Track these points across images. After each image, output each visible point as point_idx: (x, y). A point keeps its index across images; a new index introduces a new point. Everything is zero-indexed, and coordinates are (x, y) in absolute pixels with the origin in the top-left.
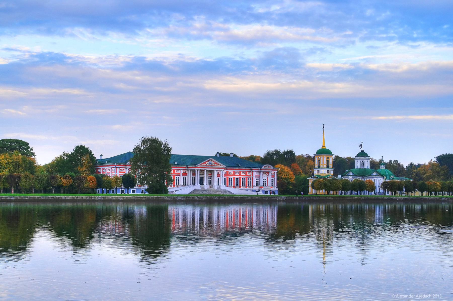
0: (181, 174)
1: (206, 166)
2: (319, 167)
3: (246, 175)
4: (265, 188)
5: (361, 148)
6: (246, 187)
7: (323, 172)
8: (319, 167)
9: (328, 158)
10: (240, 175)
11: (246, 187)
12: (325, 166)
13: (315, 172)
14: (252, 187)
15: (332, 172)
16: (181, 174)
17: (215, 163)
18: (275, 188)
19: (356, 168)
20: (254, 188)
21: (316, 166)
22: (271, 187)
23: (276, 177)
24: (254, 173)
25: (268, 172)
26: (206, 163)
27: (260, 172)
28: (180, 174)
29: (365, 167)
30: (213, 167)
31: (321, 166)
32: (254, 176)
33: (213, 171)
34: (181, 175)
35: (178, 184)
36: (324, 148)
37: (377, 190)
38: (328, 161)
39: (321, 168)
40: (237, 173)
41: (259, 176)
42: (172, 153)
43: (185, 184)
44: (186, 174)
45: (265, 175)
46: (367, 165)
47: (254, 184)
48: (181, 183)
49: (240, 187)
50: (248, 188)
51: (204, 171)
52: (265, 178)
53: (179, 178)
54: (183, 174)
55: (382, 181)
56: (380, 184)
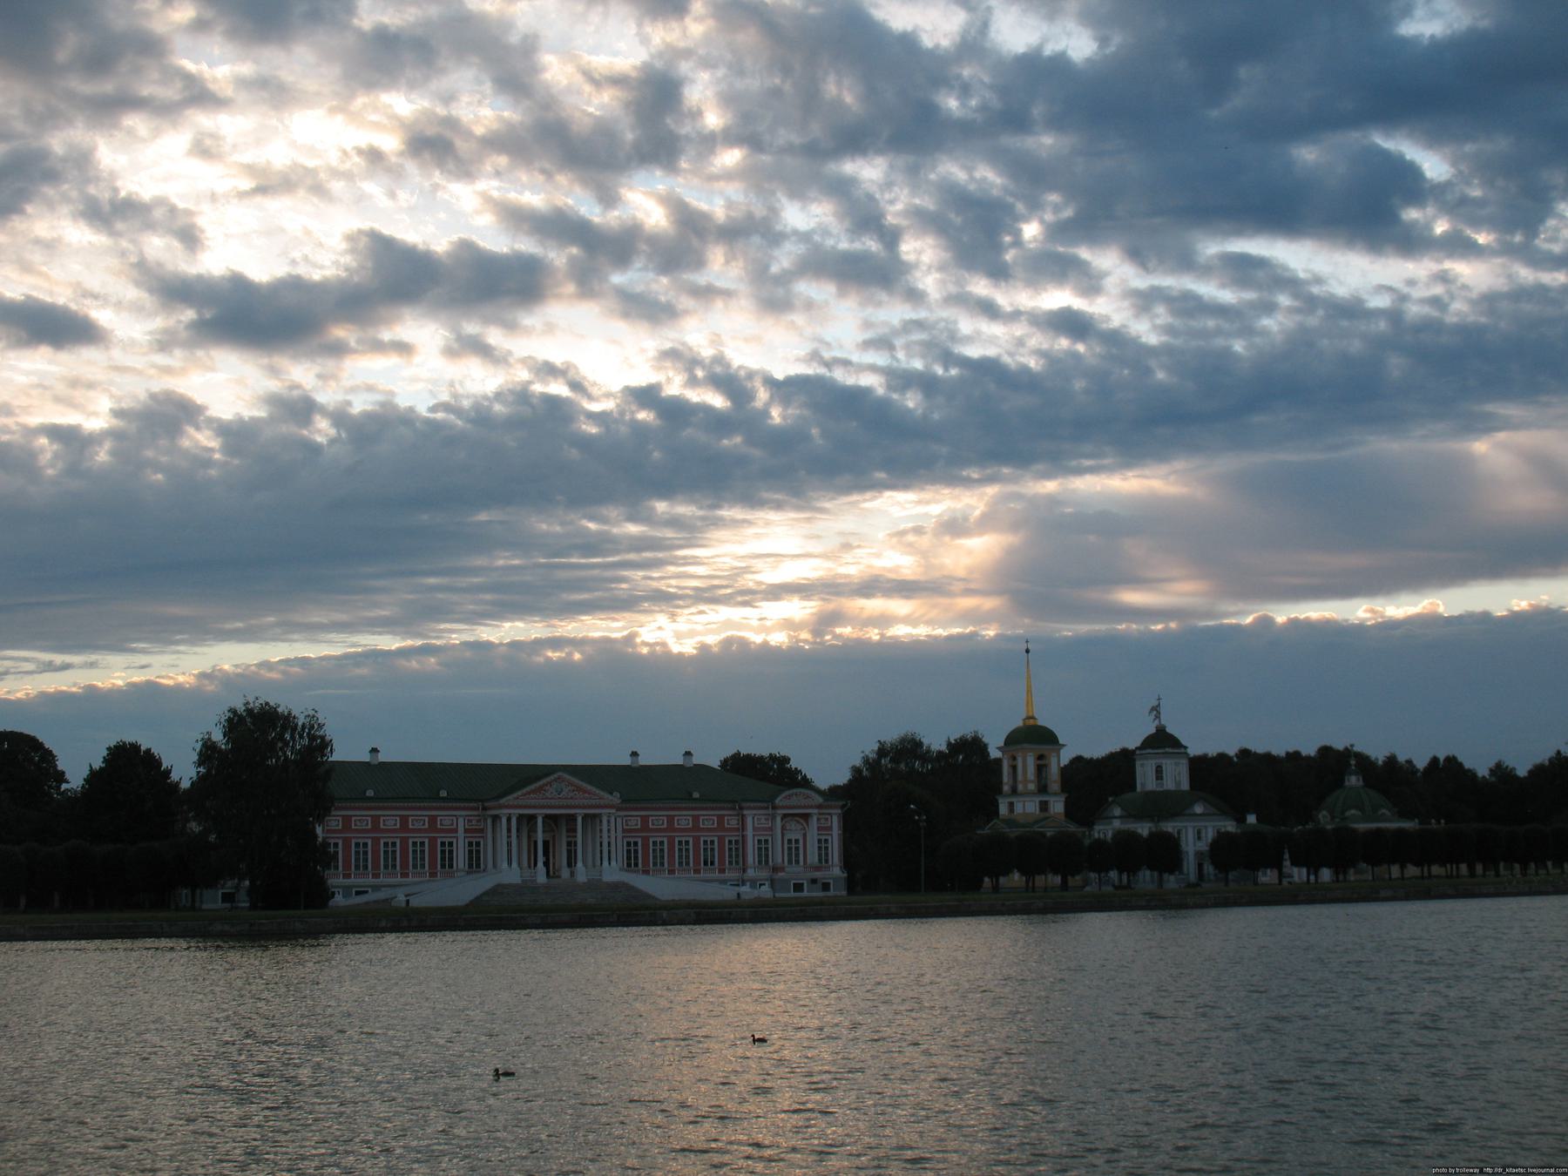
0: (461, 829)
1: (543, 802)
2: (1014, 791)
4: (794, 872)
5: (1158, 717)
6: (722, 871)
7: (1027, 807)
8: (1014, 791)
9: (1041, 757)
10: (696, 828)
11: (722, 871)
12: (1032, 787)
13: (1003, 809)
14: (744, 871)
15: (1058, 806)
16: (461, 829)
17: (579, 789)
18: (837, 871)
19: (1139, 789)
20: (751, 873)
21: (1006, 788)
22: (818, 869)
23: (836, 832)
24: (749, 821)
25: (806, 817)
26: (541, 788)
27: (774, 818)
28: (456, 831)
29: (1169, 784)
30: (570, 802)
31: (1020, 787)
32: (749, 833)
33: (600, 815)
35: (451, 866)
36: (1031, 722)
37: (1190, 865)
38: (1041, 769)
39: (1021, 794)
40: (684, 819)
41: (771, 829)
42: (340, 754)
43: (478, 866)
44: (482, 831)
45: (792, 825)
46: (1176, 776)
47: (751, 858)
49: (697, 871)
52: (793, 837)
53: (451, 844)
54: (466, 831)
55: (1210, 835)
56: (1203, 846)
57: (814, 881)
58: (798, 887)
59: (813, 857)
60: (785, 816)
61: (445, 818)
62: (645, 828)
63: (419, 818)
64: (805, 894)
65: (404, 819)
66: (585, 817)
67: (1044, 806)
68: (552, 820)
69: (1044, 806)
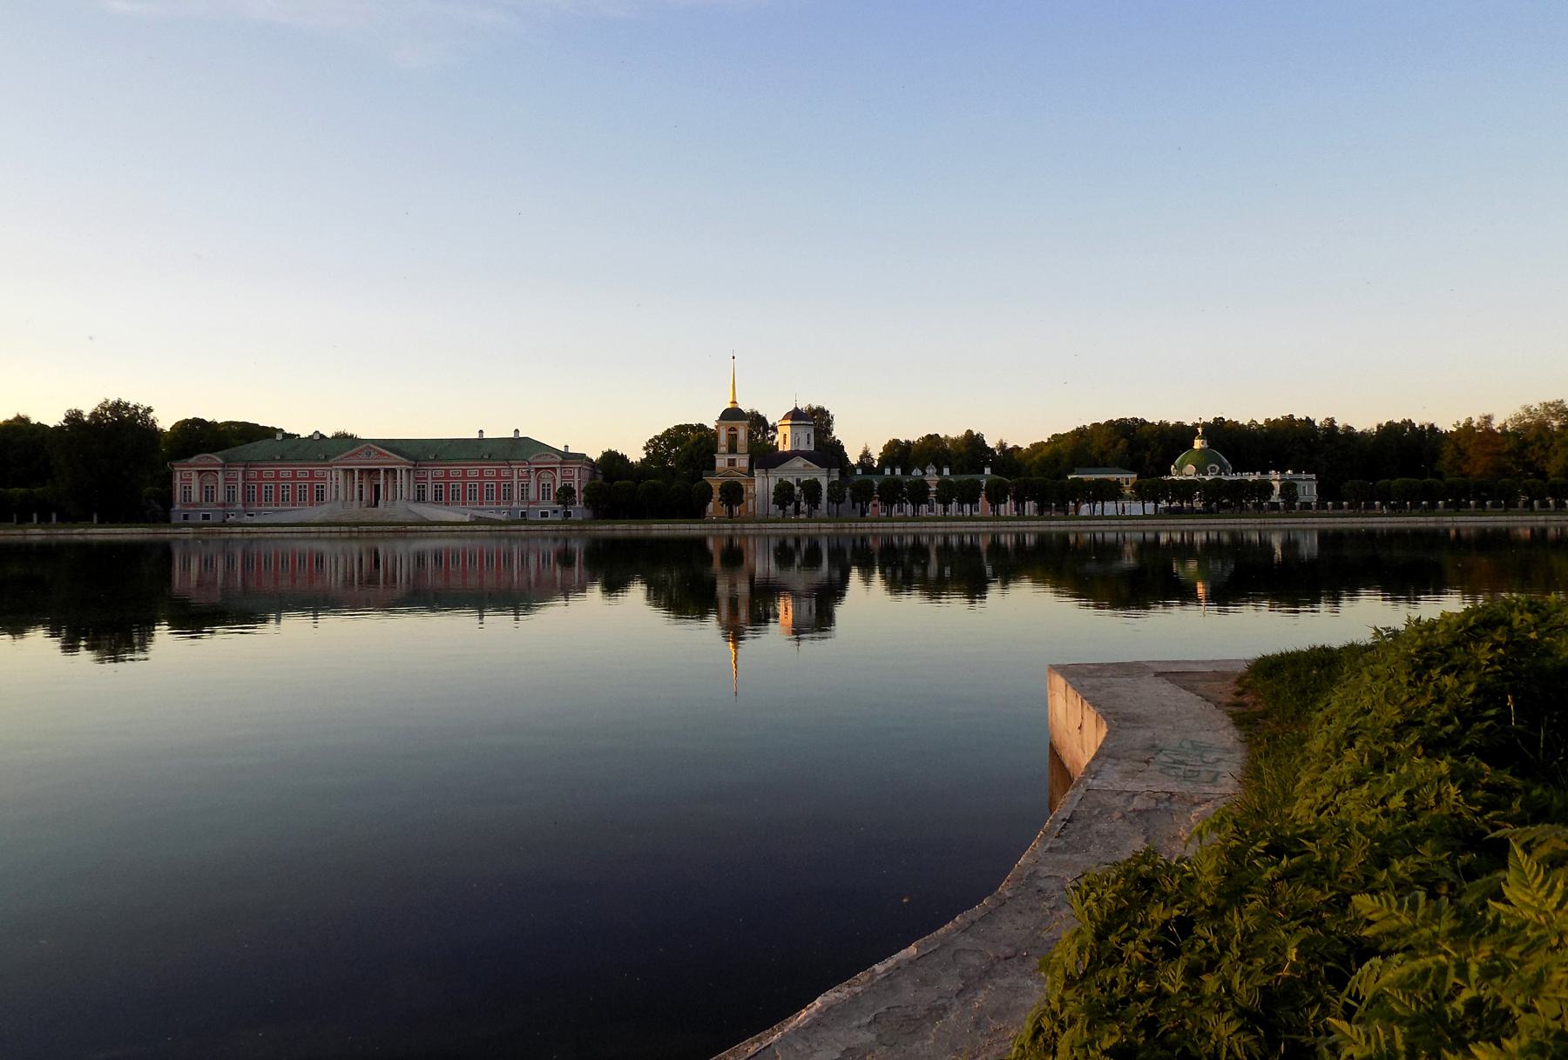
3: (499, 476)
15: (743, 462)
20: (515, 505)
25: (554, 469)
32: (515, 479)
51: (352, 471)
58: (544, 514)
62: (447, 476)
63: (303, 471)
67: (732, 463)
68: (386, 471)
69: (732, 463)
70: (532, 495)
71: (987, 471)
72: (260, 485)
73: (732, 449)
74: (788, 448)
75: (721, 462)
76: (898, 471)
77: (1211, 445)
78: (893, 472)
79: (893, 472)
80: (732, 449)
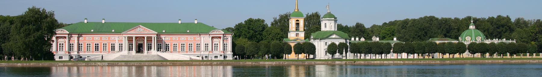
10: (187, 40)
15: (302, 35)
24: (202, 38)
25: (220, 37)
34: (117, 42)
38: (298, 24)
45: (215, 40)
48: (117, 48)
50: (196, 53)
51: (132, 37)
52: (216, 43)
57: (221, 55)
58: (216, 57)
59: (222, 49)
60: (213, 38)
61: (112, 37)
64: (218, 59)
65: (101, 38)
66: (148, 37)
69: (297, 35)
70: (210, 48)
71: (395, 39)
72: (84, 43)
73: (297, 29)
74: (328, 29)
75: (292, 35)
76: (357, 39)
77: (477, 28)
78: (355, 39)
79: (355, 39)
80: (297, 29)
